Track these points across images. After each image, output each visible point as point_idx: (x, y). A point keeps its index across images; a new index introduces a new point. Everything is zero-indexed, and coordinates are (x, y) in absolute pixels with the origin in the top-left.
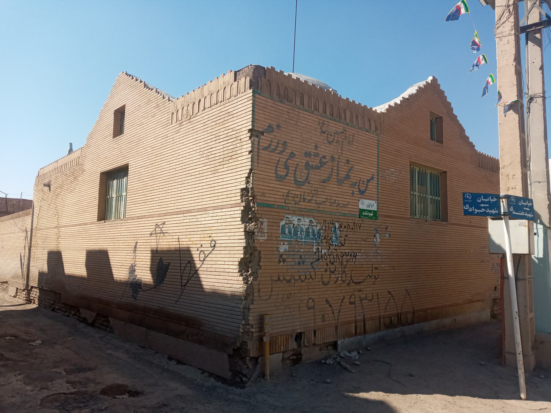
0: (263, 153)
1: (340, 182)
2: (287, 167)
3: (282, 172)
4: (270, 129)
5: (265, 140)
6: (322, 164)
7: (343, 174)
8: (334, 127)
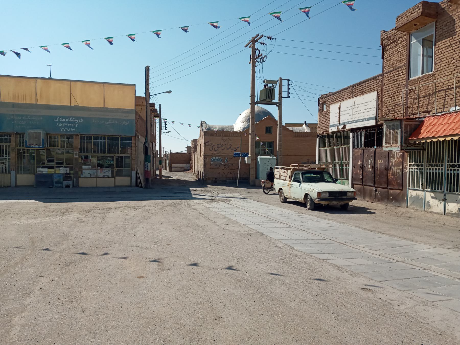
0: (207, 147)
1: (228, 149)
2: (212, 148)
3: (211, 149)
4: (208, 142)
5: (207, 144)
6: (222, 146)
7: (229, 147)
8: (225, 138)
